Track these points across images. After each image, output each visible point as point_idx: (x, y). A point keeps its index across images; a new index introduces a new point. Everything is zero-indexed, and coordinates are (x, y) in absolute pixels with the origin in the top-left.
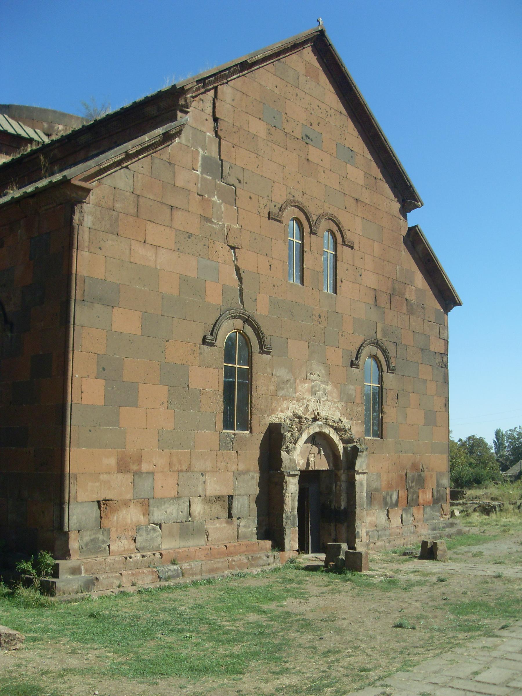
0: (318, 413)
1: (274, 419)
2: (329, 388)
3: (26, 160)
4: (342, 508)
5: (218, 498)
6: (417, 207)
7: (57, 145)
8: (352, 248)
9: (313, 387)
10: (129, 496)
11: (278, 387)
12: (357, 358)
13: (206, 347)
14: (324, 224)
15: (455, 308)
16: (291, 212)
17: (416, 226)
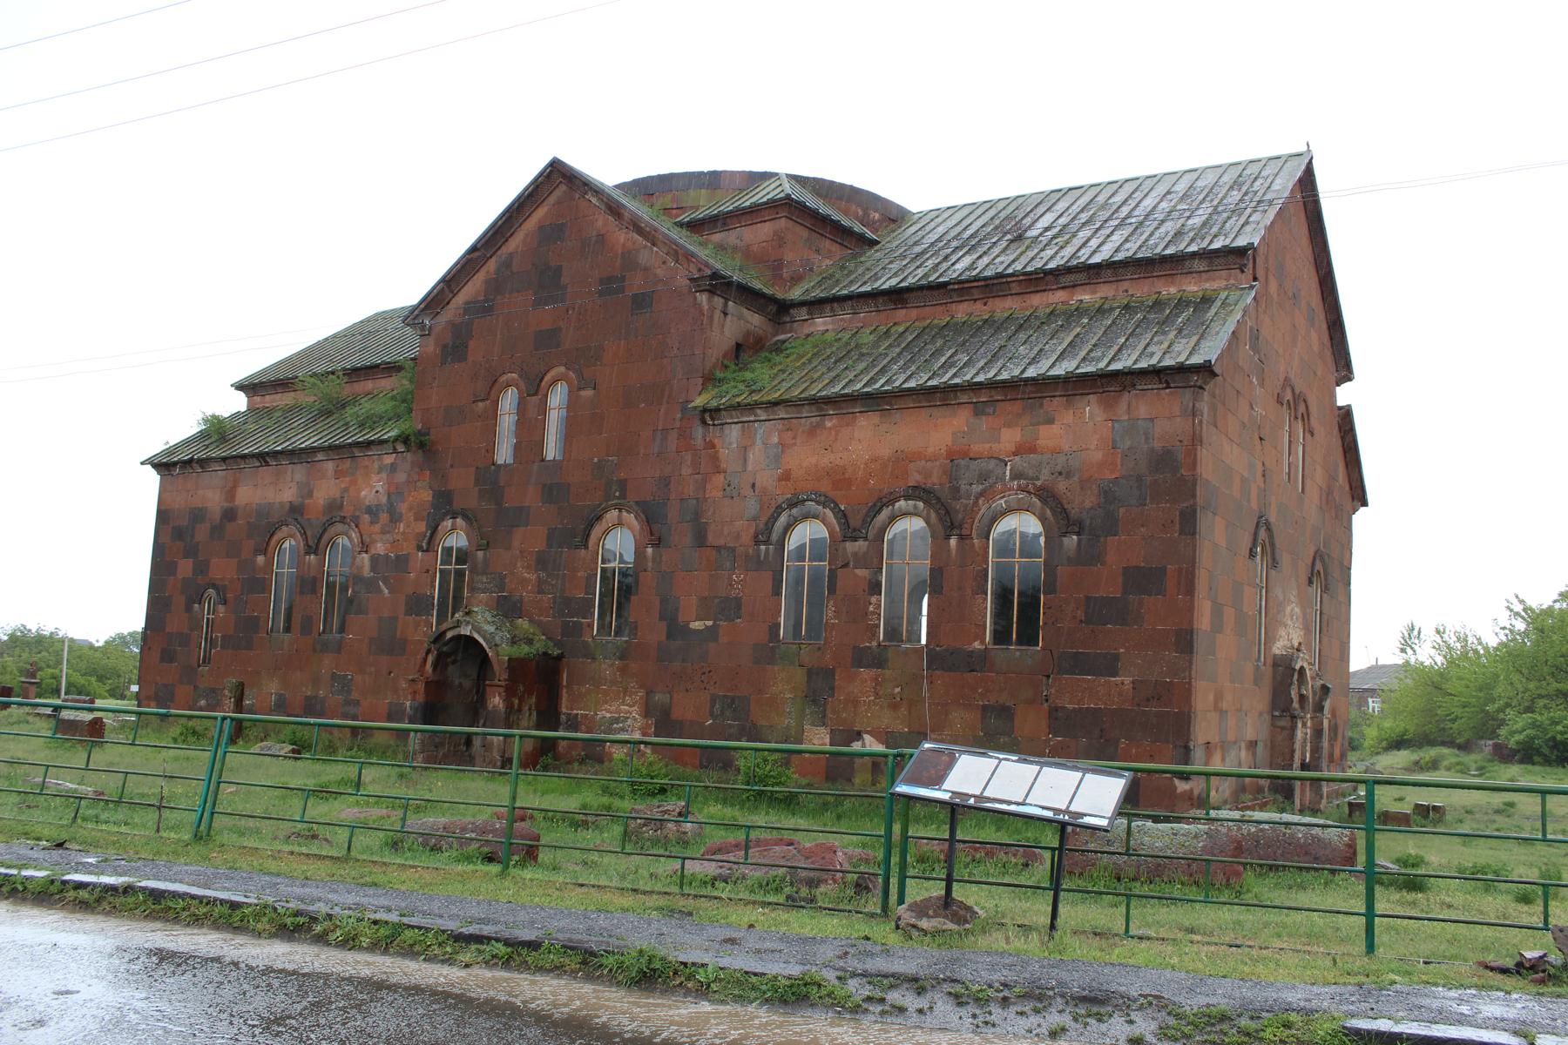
0: (1300, 644)
1: (1278, 648)
2: (1297, 610)
3: (956, 287)
4: (1307, 760)
5: (1251, 742)
6: (1350, 379)
7: (1021, 278)
8: (1312, 435)
9: (1292, 610)
10: (1216, 739)
11: (1279, 612)
12: (1312, 575)
13: (1250, 561)
14: (1302, 408)
15: (1362, 509)
16: (1288, 396)
17: (1349, 406)
